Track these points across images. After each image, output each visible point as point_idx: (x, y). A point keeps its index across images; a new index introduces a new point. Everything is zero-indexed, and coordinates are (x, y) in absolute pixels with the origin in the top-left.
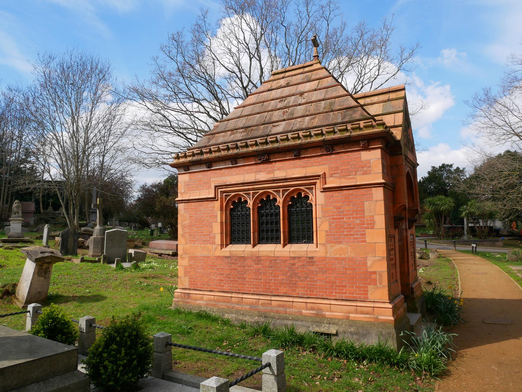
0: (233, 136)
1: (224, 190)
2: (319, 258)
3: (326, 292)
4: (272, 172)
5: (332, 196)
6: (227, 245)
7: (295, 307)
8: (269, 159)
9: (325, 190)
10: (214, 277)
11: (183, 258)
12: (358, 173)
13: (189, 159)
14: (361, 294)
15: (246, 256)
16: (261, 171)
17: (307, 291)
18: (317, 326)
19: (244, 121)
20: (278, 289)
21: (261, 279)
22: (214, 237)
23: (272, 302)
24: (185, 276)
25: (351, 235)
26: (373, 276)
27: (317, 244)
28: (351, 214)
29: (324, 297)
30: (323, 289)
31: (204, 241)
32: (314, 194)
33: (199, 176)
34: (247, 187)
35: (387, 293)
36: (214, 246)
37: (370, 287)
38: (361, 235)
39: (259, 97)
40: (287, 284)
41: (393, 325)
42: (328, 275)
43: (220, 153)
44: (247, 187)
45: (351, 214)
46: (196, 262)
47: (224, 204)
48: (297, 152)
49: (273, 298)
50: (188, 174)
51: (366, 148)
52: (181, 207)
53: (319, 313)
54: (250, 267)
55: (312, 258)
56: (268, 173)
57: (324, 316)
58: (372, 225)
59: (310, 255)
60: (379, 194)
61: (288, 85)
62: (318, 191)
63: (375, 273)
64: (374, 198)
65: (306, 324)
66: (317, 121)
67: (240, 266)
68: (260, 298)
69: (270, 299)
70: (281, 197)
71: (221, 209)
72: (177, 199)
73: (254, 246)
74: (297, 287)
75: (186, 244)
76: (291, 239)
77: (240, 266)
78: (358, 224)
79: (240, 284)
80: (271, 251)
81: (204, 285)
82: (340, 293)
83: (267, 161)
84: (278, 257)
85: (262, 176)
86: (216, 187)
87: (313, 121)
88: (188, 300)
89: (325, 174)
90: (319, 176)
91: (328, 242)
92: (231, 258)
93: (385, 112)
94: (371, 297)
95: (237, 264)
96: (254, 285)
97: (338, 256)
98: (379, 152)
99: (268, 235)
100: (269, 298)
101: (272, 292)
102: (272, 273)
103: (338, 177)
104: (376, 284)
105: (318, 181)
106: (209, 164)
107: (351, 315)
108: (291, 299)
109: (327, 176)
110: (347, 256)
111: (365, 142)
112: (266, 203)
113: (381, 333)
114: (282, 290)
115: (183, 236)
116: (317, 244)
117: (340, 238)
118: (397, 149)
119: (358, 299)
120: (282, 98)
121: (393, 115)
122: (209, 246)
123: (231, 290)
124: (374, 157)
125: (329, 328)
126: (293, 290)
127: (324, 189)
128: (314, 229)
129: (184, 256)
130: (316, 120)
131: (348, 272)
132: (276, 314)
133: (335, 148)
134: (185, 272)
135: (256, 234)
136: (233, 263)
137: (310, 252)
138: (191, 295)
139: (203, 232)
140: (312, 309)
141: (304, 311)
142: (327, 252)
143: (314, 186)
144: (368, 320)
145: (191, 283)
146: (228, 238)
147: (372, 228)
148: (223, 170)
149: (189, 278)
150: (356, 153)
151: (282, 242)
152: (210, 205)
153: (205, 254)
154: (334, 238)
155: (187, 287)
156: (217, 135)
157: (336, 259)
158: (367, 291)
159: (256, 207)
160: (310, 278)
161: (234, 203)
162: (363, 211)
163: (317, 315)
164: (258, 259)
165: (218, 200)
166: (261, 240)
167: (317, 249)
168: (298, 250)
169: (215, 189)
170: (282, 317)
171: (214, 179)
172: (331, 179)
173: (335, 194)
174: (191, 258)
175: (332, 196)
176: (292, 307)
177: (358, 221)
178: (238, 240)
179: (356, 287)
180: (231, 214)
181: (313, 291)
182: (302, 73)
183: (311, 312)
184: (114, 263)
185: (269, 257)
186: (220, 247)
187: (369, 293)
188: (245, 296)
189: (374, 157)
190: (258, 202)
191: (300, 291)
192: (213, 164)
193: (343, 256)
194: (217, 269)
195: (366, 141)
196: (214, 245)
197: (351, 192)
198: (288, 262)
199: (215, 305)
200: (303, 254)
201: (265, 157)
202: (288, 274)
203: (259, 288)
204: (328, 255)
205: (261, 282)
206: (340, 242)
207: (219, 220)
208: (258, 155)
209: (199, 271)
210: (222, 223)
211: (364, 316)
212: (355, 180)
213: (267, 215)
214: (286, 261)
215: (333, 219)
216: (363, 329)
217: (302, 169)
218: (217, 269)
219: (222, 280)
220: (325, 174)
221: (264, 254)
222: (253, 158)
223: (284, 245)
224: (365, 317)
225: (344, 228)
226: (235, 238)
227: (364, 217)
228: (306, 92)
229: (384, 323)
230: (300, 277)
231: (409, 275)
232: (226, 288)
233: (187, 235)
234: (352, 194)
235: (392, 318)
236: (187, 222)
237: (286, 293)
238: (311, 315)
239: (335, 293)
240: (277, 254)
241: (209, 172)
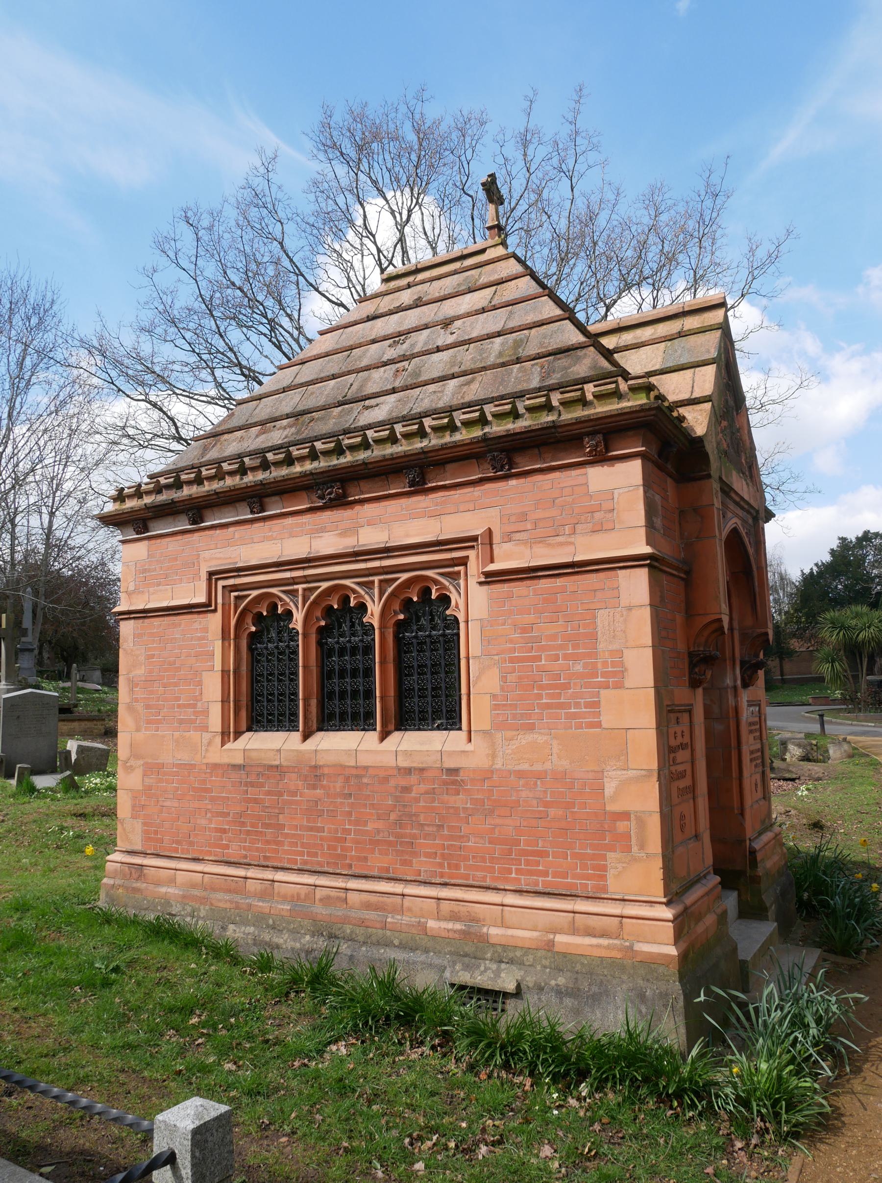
0: (262, 437)
1: (231, 582)
2: (474, 771)
3: (491, 870)
4: (352, 530)
5: (510, 596)
6: (238, 734)
7: (410, 909)
8: (345, 495)
9: (492, 578)
10: (203, 822)
11: (129, 769)
12: (579, 527)
13: (148, 500)
14: (588, 877)
15: (285, 764)
16: (323, 530)
17: (441, 865)
18: (467, 967)
19: (297, 398)
20: (366, 859)
21: (321, 830)
22: (206, 713)
23: (350, 895)
24: (134, 817)
25: (561, 706)
26: (621, 826)
27: (470, 732)
28: (561, 647)
29: (488, 883)
30: (483, 859)
31: (181, 722)
32: (462, 591)
33: (172, 545)
34: (288, 575)
35: (660, 874)
36: (206, 736)
37: (612, 857)
38: (588, 705)
39: (344, 336)
40: (390, 844)
41: (674, 969)
42: (498, 821)
43: (221, 483)
44: (288, 575)
45: (561, 647)
46: (160, 781)
47: (233, 622)
49: (353, 884)
50: (146, 542)
51: (601, 458)
52: (126, 628)
53: (472, 930)
54: (294, 794)
55: (455, 771)
56: (344, 534)
57: (484, 939)
58: (616, 678)
59: (450, 764)
60: (636, 586)
61: (418, 303)
62: (472, 582)
63: (625, 816)
64: (624, 601)
65: (437, 961)
66: (476, 390)
67: (269, 793)
68: (318, 882)
69: (342, 885)
70: (376, 599)
71: (225, 636)
72: (116, 610)
73: (306, 737)
74: (415, 854)
75: (138, 730)
76: (405, 718)
77: (269, 793)
78: (581, 676)
79: (268, 842)
80: (347, 752)
81: (178, 842)
82: (531, 873)
83: (340, 502)
84: (366, 768)
86: (211, 574)
87: (465, 389)
88: (138, 885)
89: (490, 531)
90: (474, 539)
91: (499, 726)
93: (670, 364)
94: (614, 887)
95: (262, 785)
96: (303, 845)
97: (525, 767)
98: (636, 465)
99: (341, 710)
100: (340, 883)
101: (350, 866)
102: (350, 814)
103: (524, 542)
104: (628, 849)
105: (471, 554)
106: (196, 512)
107: (560, 938)
108: (398, 888)
109: (496, 539)
110: (548, 766)
111: (599, 440)
112: (339, 616)
113: (642, 997)
114: (377, 861)
115: (130, 708)
116: (470, 732)
117: (529, 716)
118: (700, 470)
119: (579, 892)
121: (689, 373)
122: (194, 735)
123: (245, 857)
124: (621, 483)
125: (497, 973)
126: (404, 863)
127: (487, 574)
129: (132, 762)
130: (475, 386)
131: (552, 812)
132: (358, 930)
133: (518, 459)
134: (134, 807)
135: (314, 702)
136: (252, 784)
137: (451, 754)
138: (146, 871)
139: (178, 699)
140: (454, 917)
141: (432, 924)
142: (494, 756)
143: (461, 568)
144: (604, 953)
145: (147, 837)
146: (244, 714)
147: (619, 686)
148: (231, 529)
149: (145, 824)
150: (574, 473)
151: (378, 727)
152: (196, 626)
153: (184, 757)
154: (514, 717)
155: (138, 847)
156: (226, 436)
157: (520, 774)
158: (604, 868)
159: (314, 630)
160: (450, 828)
161: (258, 618)
162: (594, 636)
163: (465, 934)
164: (314, 774)
165: (215, 610)
166: (331, 717)
167: (470, 747)
168: (417, 747)
169: (209, 580)
170: (374, 939)
171: (206, 554)
172: (507, 546)
175: (510, 596)
176: (401, 910)
177: (579, 668)
178: (269, 721)
179: (574, 855)
180: (251, 649)
181: (457, 867)
183: (450, 925)
184: (13, 776)
185: (343, 767)
186: (218, 739)
187: (611, 874)
188: (280, 876)
189: (621, 483)
190: (318, 613)
191: (423, 865)
192: (207, 513)
193: (538, 767)
194: (212, 799)
195: (600, 437)
196: (204, 734)
197: (559, 582)
198: (392, 783)
199: (203, 900)
200: (431, 761)
201: (336, 489)
202: (393, 816)
203: (316, 855)
204: (499, 764)
205: (322, 839)
206: (531, 728)
207: (218, 666)
208: (317, 484)
209: (168, 803)
210: (225, 673)
211: (594, 941)
212: (571, 549)
213: (342, 652)
214: (386, 780)
215: (512, 660)
216: (588, 981)
217: (432, 521)
218: (212, 799)
219: (224, 831)
220: (490, 531)
221: (331, 759)
222: (304, 494)
223: (384, 735)
224: (599, 946)
225: (542, 688)
226: (262, 715)
227: (594, 655)
228: (459, 318)
229: (650, 963)
230: (422, 825)
231: (742, 814)
232: (234, 851)
233: (139, 706)
234: (563, 590)
235: (673, 951)
236: (140, 672)
237: (387, 870)
238: (451, 935)
239: (518, 871)
240: (364, 760)
241: (196, 536)
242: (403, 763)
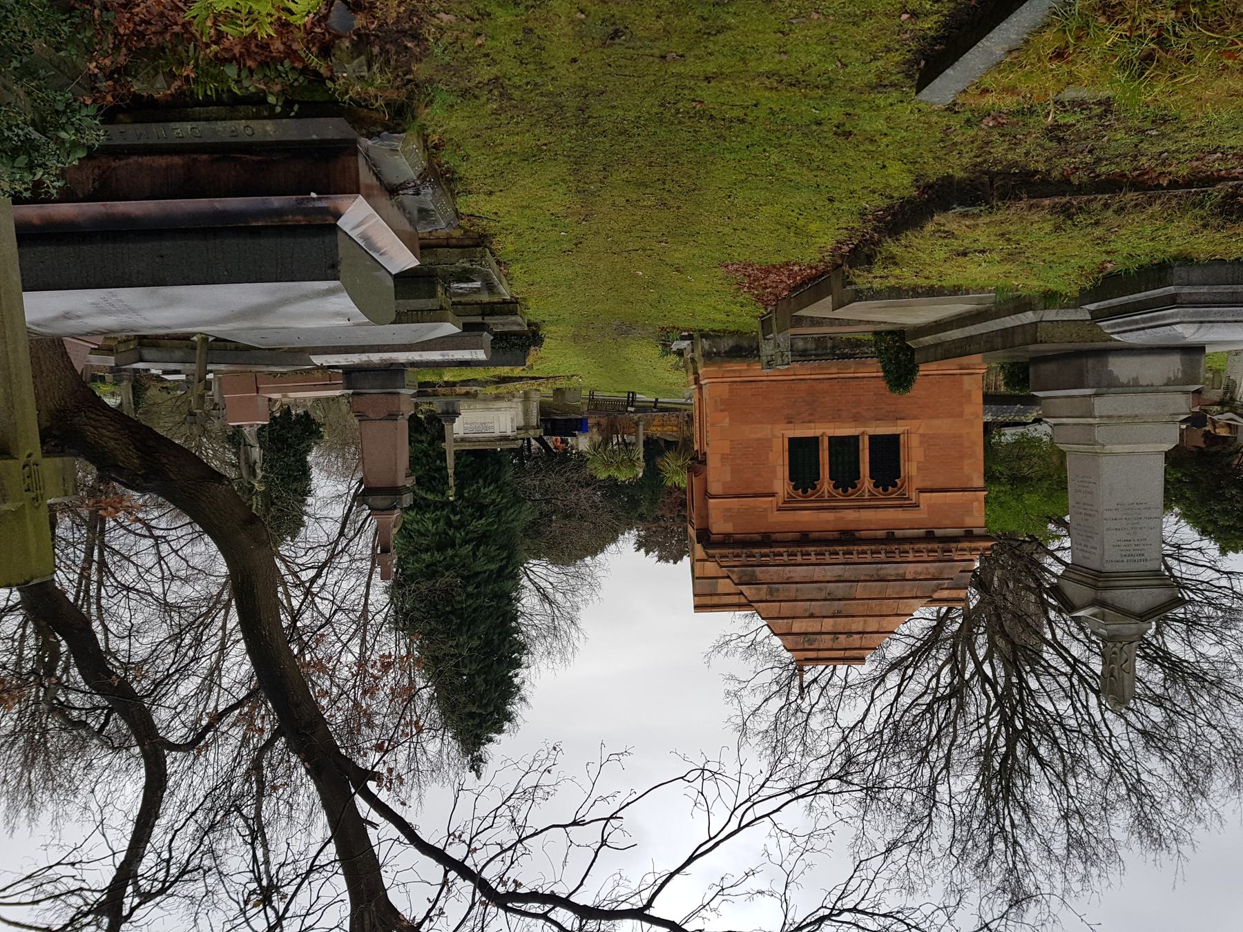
9: (773, 495)
22: (921, 443)
36: (921, 431)
48: (804, 539)
51: (728, 535)
52: (979, 482)
58: (724, 457)
60: (714, 488)
62: (781, 494)
83: (843, 532)
85: (850, 515)
92: (897, 418)
94: (726, 386)
99: (844, 448)
111: (727, 541)
128: (786, 454)
134: (970, 396)
155: (965, 377)
157: (761, 423)
164: (856, 419)
173: (760, 490)
174: (961, 415)
182: (819, 650)
189: (719, 526)
201: (847, 537)
206: (757, 440)
240: (832, 425)
242: (812, 425)
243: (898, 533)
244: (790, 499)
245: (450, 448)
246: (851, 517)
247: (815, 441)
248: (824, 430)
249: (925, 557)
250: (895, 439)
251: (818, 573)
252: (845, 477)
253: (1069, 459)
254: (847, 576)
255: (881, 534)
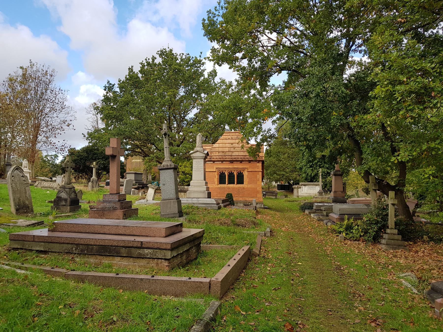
48: (241, 162)
51: (258, 163)
60: (261, 173)
85: (230, 167)
99: (231, 182)
120: (232, 144)
124: (260, 165)
164: (229, 188)
201: (232, 162)
243: (221, 162)
244: (243, 170)
245: (320, 183)
246: (230, 166)
247: (238, 183)
248: (235, 186)
249: (215, 157)
250: (220, 184)
251: (237, 154)
252: (231, 175)
253: (203, 179)
254: (231, 153)
255: (224, 162)
